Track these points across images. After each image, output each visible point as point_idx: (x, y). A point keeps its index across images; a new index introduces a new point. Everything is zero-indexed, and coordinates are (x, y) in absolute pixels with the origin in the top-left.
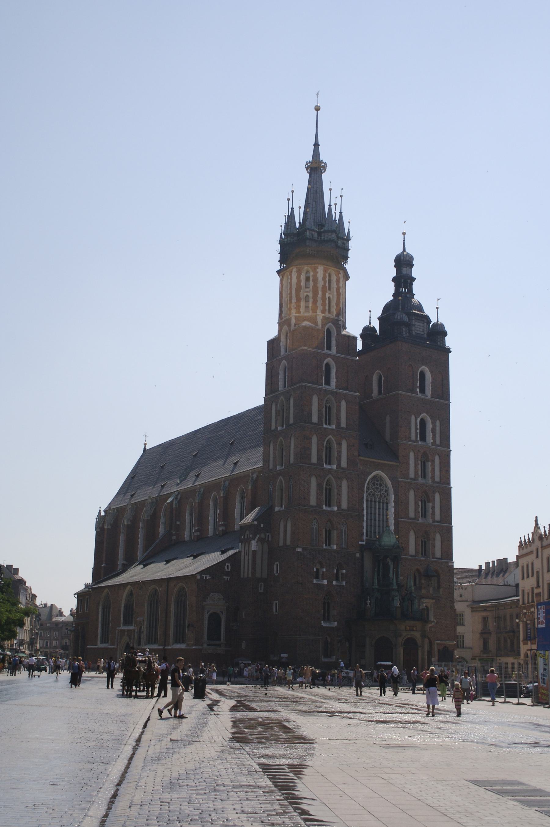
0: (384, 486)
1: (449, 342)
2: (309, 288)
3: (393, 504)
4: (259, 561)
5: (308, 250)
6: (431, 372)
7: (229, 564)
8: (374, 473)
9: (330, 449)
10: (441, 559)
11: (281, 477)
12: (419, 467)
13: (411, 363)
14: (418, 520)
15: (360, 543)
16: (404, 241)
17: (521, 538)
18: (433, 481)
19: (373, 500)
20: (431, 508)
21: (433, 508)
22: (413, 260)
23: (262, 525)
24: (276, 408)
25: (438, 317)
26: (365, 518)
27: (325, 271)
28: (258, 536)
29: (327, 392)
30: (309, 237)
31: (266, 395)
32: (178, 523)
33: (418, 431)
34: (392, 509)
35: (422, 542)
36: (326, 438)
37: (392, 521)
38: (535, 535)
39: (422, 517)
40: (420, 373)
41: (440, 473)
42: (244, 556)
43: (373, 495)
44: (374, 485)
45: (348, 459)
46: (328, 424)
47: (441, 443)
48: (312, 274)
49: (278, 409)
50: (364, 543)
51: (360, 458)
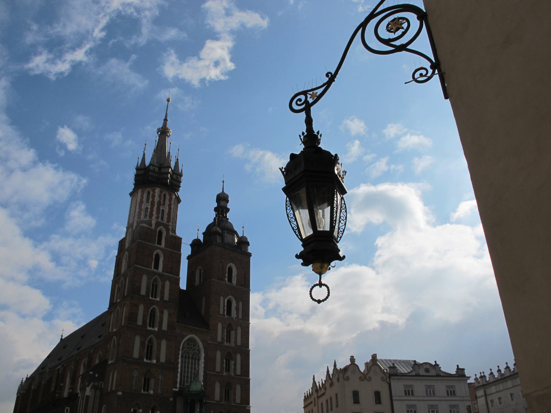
0: (196, 347)
1: (250, 249)
2: (149, 203)
3: (203, 361)
4: (90, 405)
5: (150, 178)
6: (237, 268)
7: (69, 408)
8: (189, 336)
9: (154, 316)
10: (240, 404)
11: (115, 337)
12: (225, 334)
14: (223, 373)
15: (174, 389)
16: (223, 186)
17: (305, 393)
21: (235, 365)
23: (97, 375)
24: (118, 286)
25: (243, 233)
26: (179, 370)
27: (161, 192)
28: (92, 383)
29: (154, 274)
32: (62, 384)
33: (226, 308)
34: (202, 365)
35: (225, 390)
36: (151, 307)
37: (201, 373)
38: (313, 389)
39: (226, 371)
40: (228, 268)
41: (241, 339)
42: (81, 400)
43: (188, 353)
44: (189, 345)
45: (168, 324)
47: (242, 317)
48: (151, 193)
49: (119, 287)
50: (177, 390)
51: (177, 324)
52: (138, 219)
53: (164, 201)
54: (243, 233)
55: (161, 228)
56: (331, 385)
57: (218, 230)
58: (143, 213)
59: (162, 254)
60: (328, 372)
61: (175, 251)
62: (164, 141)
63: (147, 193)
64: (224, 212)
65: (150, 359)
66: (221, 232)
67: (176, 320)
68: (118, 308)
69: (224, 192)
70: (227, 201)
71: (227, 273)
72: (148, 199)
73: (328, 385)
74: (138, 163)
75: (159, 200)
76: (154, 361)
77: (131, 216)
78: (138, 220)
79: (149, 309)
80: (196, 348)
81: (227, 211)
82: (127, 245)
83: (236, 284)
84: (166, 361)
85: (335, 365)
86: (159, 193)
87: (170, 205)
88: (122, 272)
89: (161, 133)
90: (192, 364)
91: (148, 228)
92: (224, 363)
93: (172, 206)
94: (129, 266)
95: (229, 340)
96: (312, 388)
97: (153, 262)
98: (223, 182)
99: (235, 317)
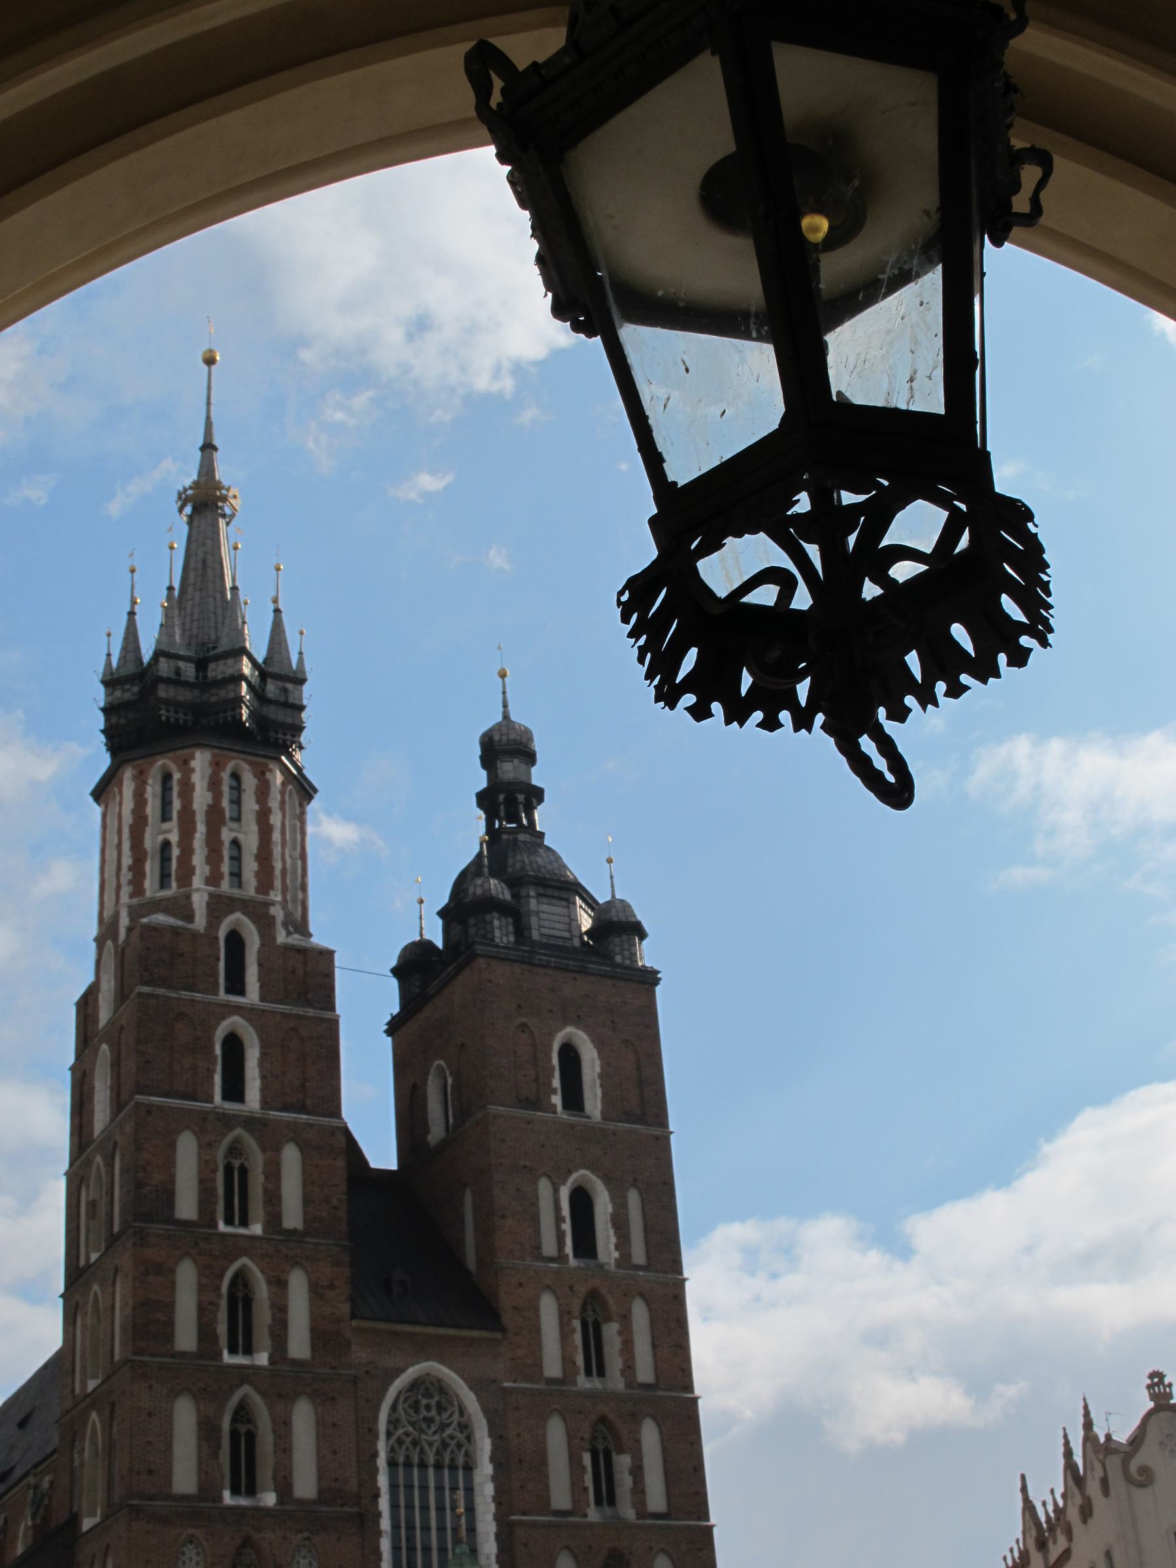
0: (453, 1413)
2: (170, 819)
5: (163, 712)
6: (599, 1044)
8: (412, 1373)
9: (248, 1302)
12: (578, 1338)
13: (524, 1020)
14: (586, 1516)
16: (504, 693)
18: (631, 1382)
19: (416, 1460)
20: (631, 1473)
21: (637, 1471)
22: (531, 739)
25: (612, 887)
26: (385, 1524)
27: (217, 765)
29: (227, 1121)
30: (165, 675)
31: (71, 1164)
33: (567, 1227)
34: (486, 1490)
36: (227, 1268)
37: (487, 1526)
41: (655, 1355)
43: (415, 1443)
44: (417, 1411)
46: (237, 1221)
47: (648, 1257)
48: (177, 776)
49: (91, 1198)
51: (354, 1323)
52: (131, 896)
53: (237, 802)
54: (612, 887)
55: (237, 922)
56: (1086, 1512)
57: (493, 892)
58: (151, 868)
59: (252, 1031)
60: (1068, 1453)
61: (311, 1012)
62: (209, 542)
63: (159, 779)
64: (521, 806)
65: (251, 1491)
66: (507, 896)
67: (345, 1308)
68: (96, 1287)
69: (513, 718)
70: (530, 758)
71: (557, 1074)
72: (166, 804)
73: (1073, 1515)
74: (109, 655)
75: (211, 802)
76: (269, 1499)
77: (107, 885)
78: (135, 901)
79: (221, 1276)
80: (450, 1416)
81: (534, 801)
82: (104, 1015)
83: (602, 1113)
84: (320, 1492)
85: (1088, 1425)
86: (209, 771)
87: (263, 816)
88: (96, 1133)
89: (194, 509)
90: (440, 1489)
91: (176, 931)
92: (584, 1468)
93: (276, 819)
94: (118, 1104)
95: (596, 1364)
96: (1024, 1533)
97: (214, 1071)
98: (503, 675)
99: (613, 1262)
